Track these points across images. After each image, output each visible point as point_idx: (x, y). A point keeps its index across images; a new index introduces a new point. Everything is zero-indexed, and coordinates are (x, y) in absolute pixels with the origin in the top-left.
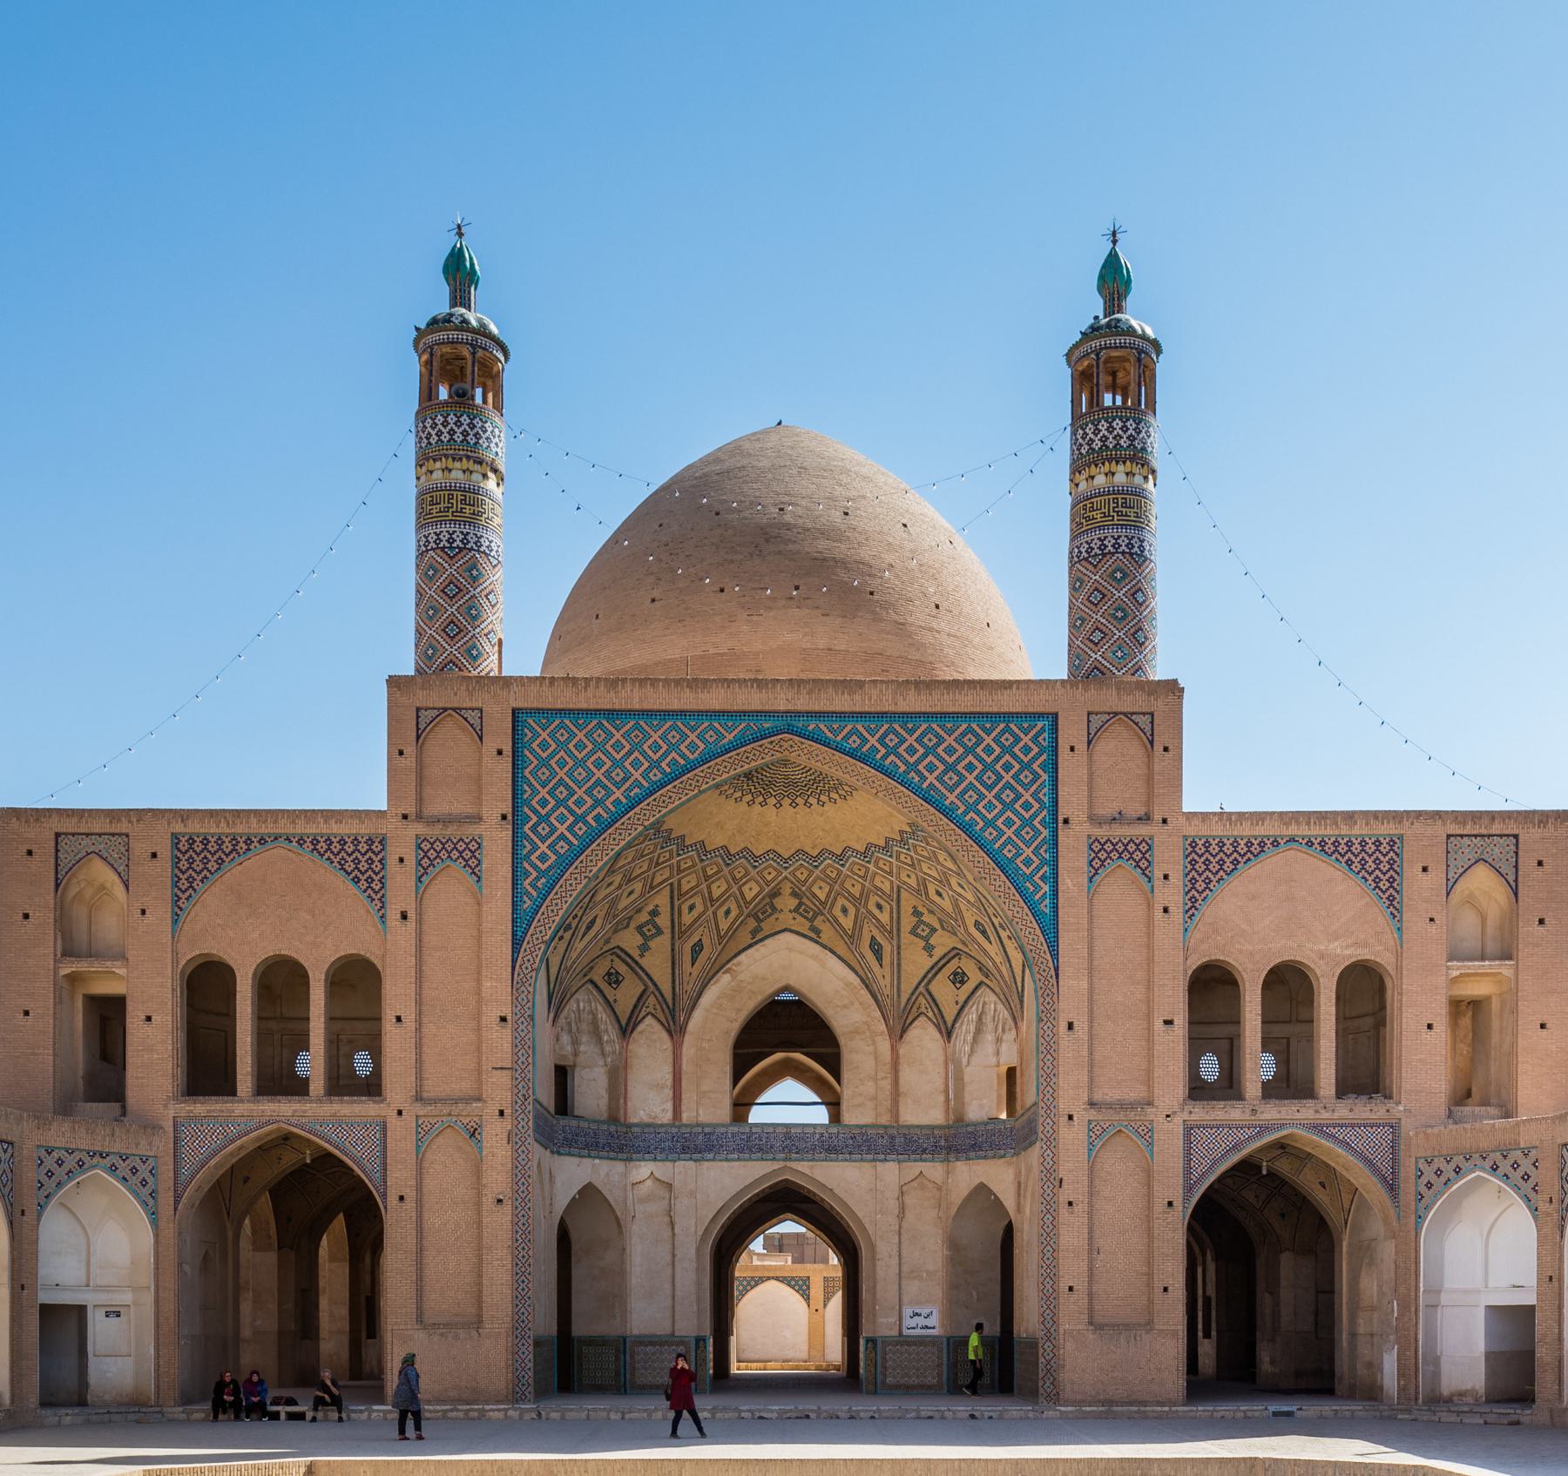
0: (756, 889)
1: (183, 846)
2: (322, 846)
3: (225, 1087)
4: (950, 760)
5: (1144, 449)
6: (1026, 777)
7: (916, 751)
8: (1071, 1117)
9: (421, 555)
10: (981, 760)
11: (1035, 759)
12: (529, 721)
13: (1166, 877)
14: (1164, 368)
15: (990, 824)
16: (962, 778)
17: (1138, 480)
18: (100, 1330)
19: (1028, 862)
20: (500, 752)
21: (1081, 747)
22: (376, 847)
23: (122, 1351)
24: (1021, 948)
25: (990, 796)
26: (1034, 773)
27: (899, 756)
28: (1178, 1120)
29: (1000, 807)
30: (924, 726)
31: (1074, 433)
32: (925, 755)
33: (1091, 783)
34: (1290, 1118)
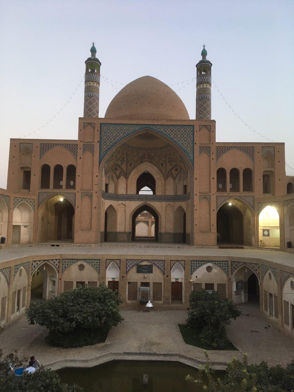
0: (141, 154)
1: (42, 145)
2: (66, 146)
3: (48, 187)
5: (209, 81)
6: (189, 136)
8: (196, 194)
9: (85, 97)
10: (181, 133)
11: (190, 133)
12: (103, 124)
13: (213, 153)
14: (213, 68)
15: (182, 144)
17: (208, 86)
18: (23, 230)
20: (98, 130)
21: (198, 131)
22: (76, 146)
23: (25, 235)
25: (182, 139)
26: (190, 135)
27: (166, 132)
28: (215, 196)
31: (197, 78)
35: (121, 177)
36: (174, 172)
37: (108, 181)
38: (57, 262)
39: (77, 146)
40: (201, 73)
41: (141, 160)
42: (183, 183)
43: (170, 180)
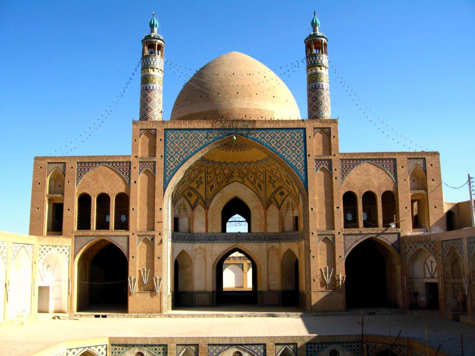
3: (89, 228)
4: (278, 140)
6: (298, 144)
7: (269, 138)
8: (313, 233)
9: (142, 91)
11: (300, 140)
13: (336, 170)
15: (289, 156)
16: (281, 145)
19: (299, 166)
21: (312, 136)
24: (298, 188)
29: (291, 152)
30: (271, 132)
32: (271, 139)
33: (315, 145)
34: (371, 231)
35: (197, 207)
36: (278, 197)
37: (178, 213)
38: (103, 350)
39: (130, 163)
40: (311, 51)
41: (228, 180)
42: (293, 213)
43: (273, 210)
